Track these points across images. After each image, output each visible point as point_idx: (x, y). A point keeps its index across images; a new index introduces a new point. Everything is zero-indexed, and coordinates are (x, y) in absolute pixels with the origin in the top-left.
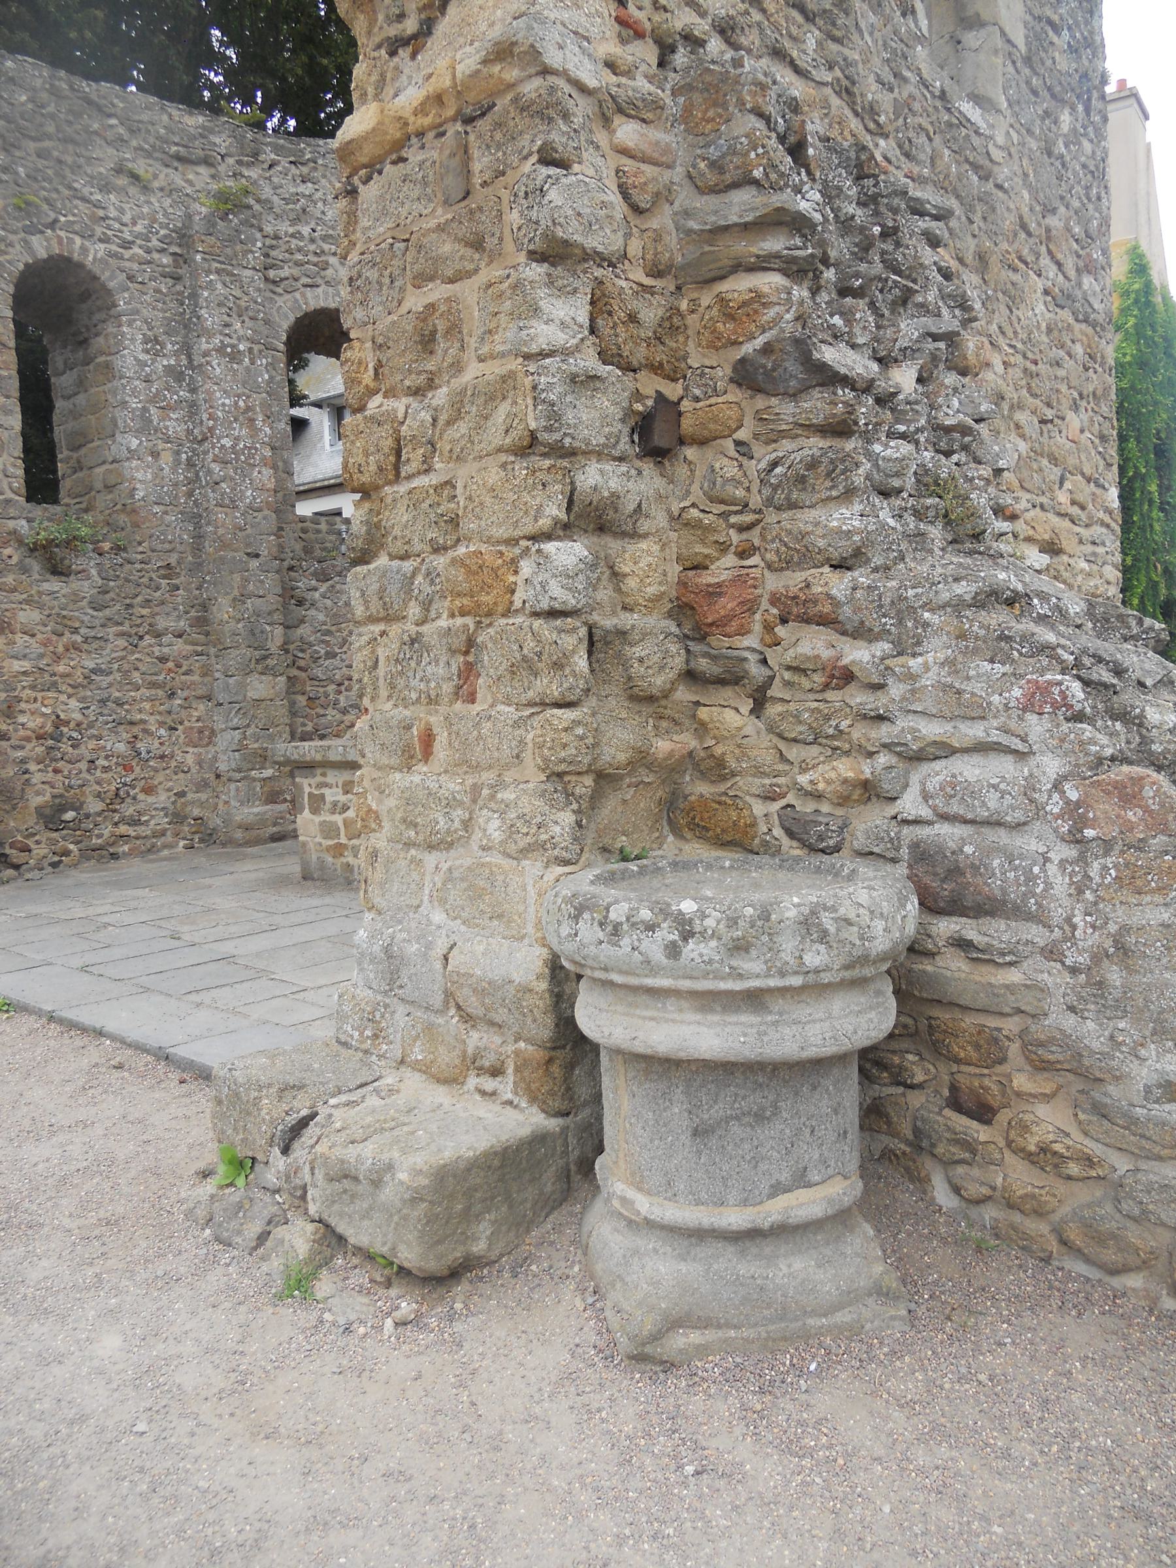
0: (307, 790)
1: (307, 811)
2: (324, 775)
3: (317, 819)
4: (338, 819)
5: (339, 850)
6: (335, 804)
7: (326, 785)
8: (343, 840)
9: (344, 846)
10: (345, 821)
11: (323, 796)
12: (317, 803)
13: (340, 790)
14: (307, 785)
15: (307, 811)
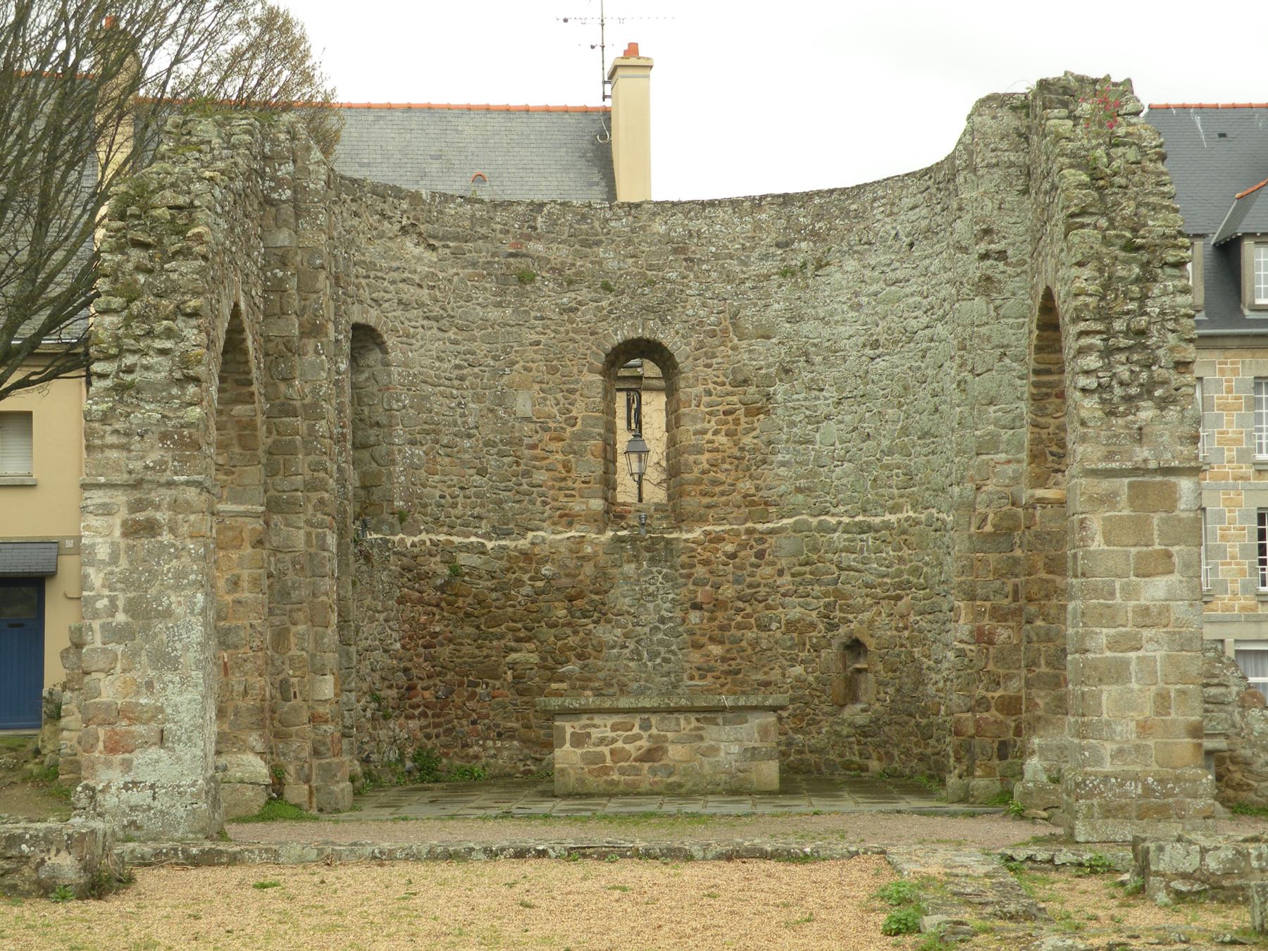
0: (569, 731)
1: (568, 745)
2: (592, 719)
3: (579, 751)
4: (606, 750)
5: (606, 770)
6: (602, 741)
7: (595, 726)
8: (609, 763)
9: (611, 768)
10: (612, 752)
11: (589, 735)
12: (578, 740)
13: (608, 729)
14: (569, 727)
15: (568, 745)
